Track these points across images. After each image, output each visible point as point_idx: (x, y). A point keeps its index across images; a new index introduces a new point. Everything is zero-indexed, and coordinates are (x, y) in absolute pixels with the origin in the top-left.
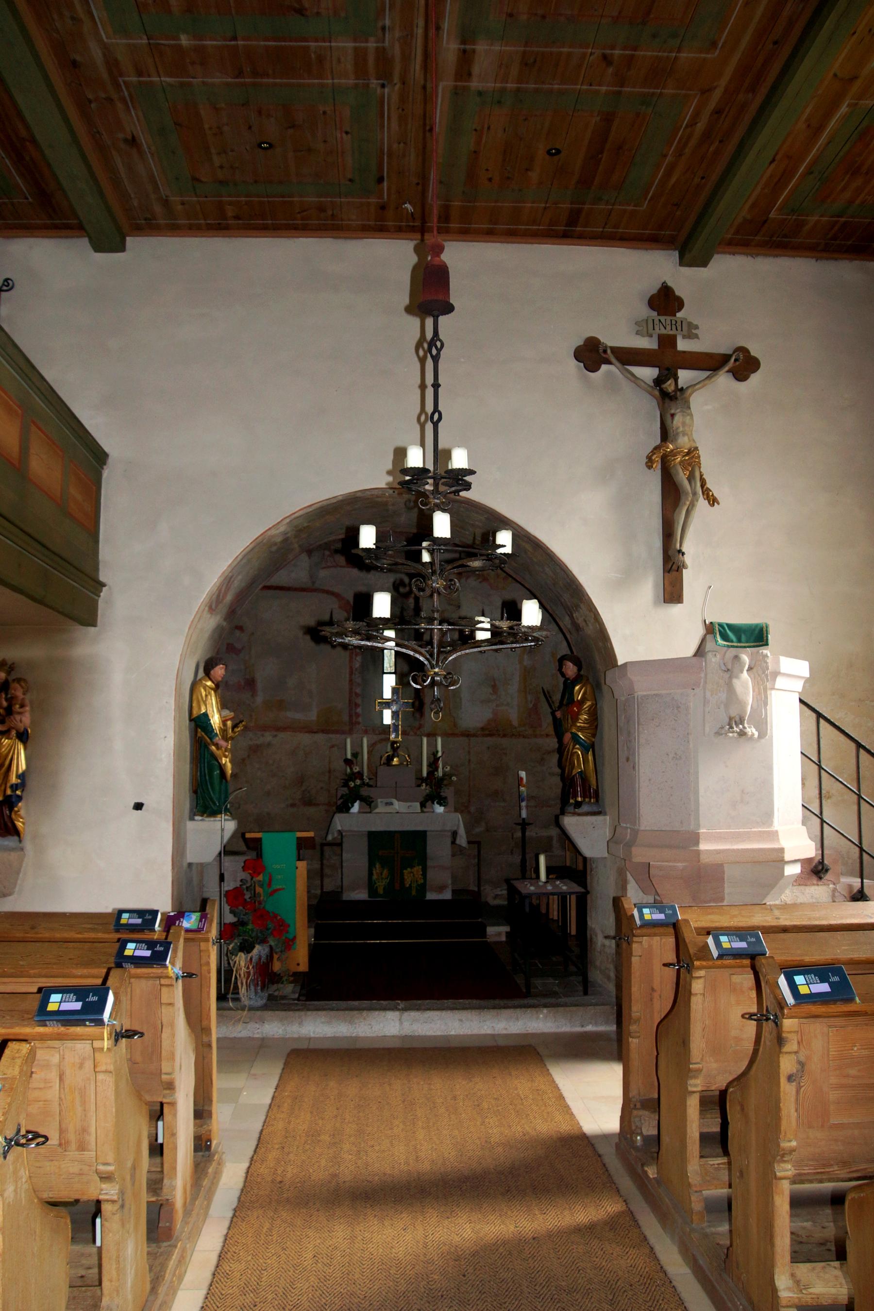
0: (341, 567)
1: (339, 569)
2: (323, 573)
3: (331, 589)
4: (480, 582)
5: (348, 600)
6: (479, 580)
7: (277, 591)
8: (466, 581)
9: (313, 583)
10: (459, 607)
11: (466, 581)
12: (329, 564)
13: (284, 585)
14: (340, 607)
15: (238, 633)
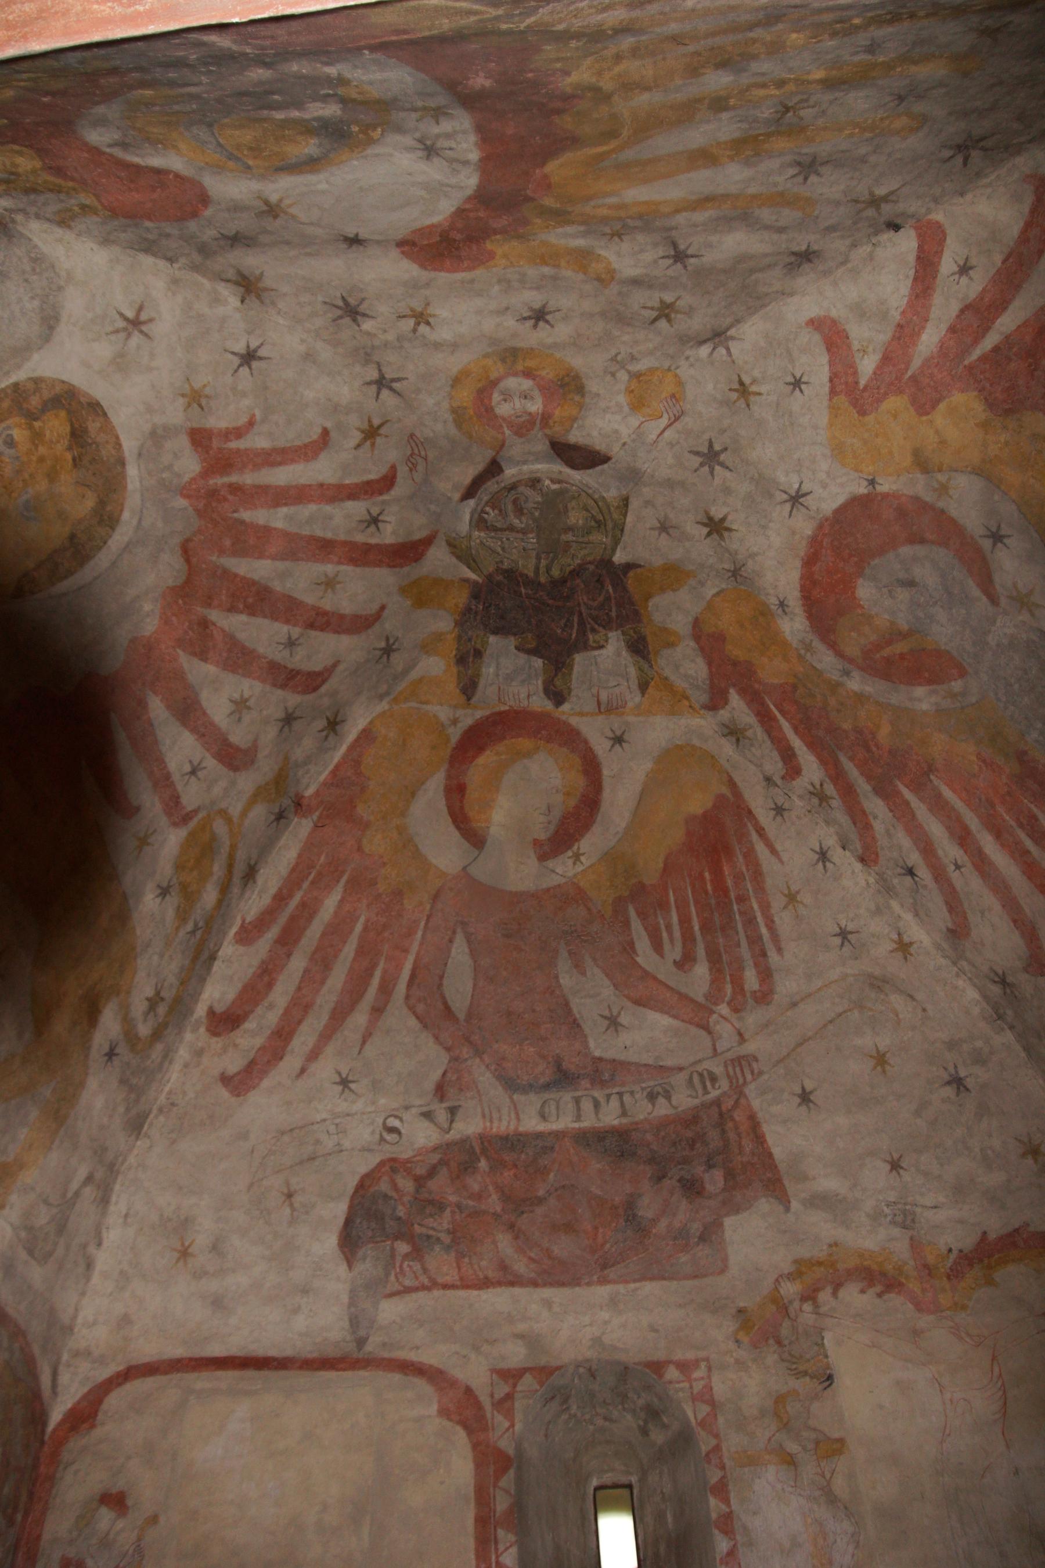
0: (446, 1287)
1: (436, 1293)
2: (390, 1311)
3: (413, 1356)
4: (880, 1295)
5: (469, 1391)
6: (879, 1288)
7: (250, 1373)
8: (835, 1294)
9: (361, 1342)
10: (830, 1378)
11: (835, 1294)
12: (408, 1282)
13: (273, 1353)
14: (444, 1412)
15: (105, 1517)
